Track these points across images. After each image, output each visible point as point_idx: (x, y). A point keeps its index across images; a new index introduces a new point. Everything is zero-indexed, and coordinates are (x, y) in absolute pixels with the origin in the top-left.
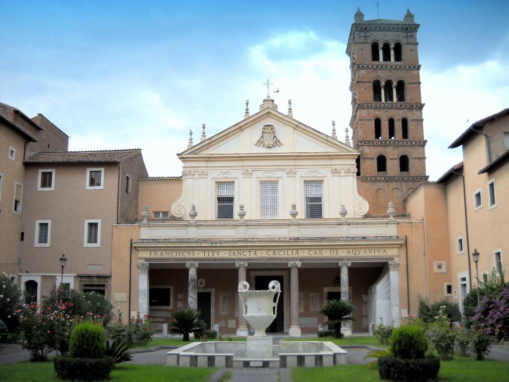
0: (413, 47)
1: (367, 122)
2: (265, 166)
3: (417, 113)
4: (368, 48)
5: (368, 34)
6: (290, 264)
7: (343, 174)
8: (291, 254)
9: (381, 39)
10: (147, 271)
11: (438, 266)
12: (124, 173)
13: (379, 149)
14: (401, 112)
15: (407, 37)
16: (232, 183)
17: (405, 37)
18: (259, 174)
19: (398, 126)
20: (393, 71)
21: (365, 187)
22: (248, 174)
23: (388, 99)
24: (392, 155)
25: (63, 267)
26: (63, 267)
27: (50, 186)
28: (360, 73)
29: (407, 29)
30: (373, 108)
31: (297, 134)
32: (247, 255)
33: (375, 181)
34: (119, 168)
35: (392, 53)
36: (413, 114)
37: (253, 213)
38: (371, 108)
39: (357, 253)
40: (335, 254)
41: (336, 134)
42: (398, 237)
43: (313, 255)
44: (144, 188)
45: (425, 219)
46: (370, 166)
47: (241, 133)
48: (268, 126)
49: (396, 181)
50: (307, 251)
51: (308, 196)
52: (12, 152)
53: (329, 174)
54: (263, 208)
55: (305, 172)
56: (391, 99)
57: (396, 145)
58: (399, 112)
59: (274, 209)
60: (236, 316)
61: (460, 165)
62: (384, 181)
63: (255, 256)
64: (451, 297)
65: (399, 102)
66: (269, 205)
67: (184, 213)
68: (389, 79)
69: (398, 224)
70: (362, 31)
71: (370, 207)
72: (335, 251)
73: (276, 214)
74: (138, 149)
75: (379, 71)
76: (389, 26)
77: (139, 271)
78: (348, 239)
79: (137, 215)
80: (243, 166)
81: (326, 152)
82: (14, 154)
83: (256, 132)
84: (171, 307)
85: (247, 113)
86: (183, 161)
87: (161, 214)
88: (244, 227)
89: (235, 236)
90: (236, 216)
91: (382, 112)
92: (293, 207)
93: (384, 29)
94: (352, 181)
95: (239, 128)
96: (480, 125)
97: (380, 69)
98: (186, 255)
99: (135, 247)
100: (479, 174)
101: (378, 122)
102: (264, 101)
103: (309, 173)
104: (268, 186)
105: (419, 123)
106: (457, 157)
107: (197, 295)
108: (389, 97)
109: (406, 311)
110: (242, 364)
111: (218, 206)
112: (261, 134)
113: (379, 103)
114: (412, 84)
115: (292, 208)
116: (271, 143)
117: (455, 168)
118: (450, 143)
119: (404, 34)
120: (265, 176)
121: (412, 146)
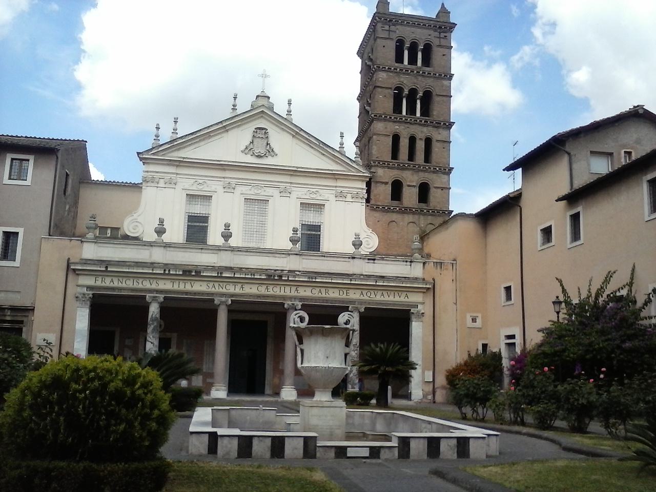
0: (445, 51)
1: (382, 138)
2: (253, 180)
3: (443, 133)
5: (393, 28)
7: (349, 198)
9: (409, 36)
10: (89, 303)
11: (472, 320)
12: (63, 167)
13: (396, 173)
14: (425, 129)
15: (440, 38)
16: (208, 198)
17: (438, 38)
18: (245, 189)
19: (420, 146)
20: (420, 78)
21: (375, 217)
22: (229, 188)
24: (410, 182)
29: (440, 27)
31: (296, 144)
32: (231, 289)
33: (388, 212)
34: (57, 158)
36: (440, 134)
38: (390, 120)
39: (373, 296)
40: (344, 296)
41: (344, 149)
42: (424, 279)
43: (316, 295)
44: (86, 194)
46: (383, 193)
47: (224, 135)
48: (260, 128)
49: (414, 213)
50: (311, 288)
51: (304, 223)
53: (332, 198)
55: (303, 193)
57: (417, 170)
60: (280, 368)
61: (516, 193)
62: (397, 212)
63: (241, 292)
66: (255, 230)
68: (414, 87)
70: (386, 24)
72: (345, 292)
74: (83, 141)
75: (401, 76)
76: (420, 21)
77: (78, 304)
78: (362, 277)
79: (75, 228)
81: (332, 170)
83: (243, 136)
85: (234, 109)
86: (144, 163)
87: (109, 231)
88: (230, 252)
89: (217, 263)
91: (403, 127)
92: (294, 231)
93: (414, 25)
94: (359, 209)
95: (224, 127)
96: (564, 139)
98: (147, 285)
99: (74, 270)
100: (556, 201)
101: (396, 139)
102: (258, 96)
103: (308, 193)
105: (445, 144)
106: (513, 183)
107: (158, 340)
108: (411, 110)
109: (431, 373)
110: (332, 454)
111: (188, 225)
112: (250, 139)
116: (263, 151)
117: (511, 196)
119: (437, 34)
120: (251, 192)
121: (435, 172)
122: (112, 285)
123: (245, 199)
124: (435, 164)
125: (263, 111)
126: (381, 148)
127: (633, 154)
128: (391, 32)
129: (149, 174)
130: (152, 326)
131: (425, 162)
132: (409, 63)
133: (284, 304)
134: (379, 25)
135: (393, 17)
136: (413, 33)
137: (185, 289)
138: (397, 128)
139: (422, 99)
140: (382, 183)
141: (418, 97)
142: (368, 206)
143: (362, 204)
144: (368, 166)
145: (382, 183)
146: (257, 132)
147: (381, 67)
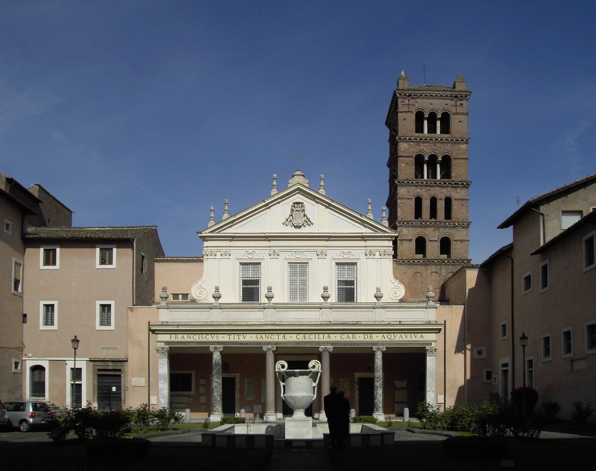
1: (405, 201)
4: (412, 117)
5: (412, 101)
6: (321, 348)
8: (321, 338)
14: (444, 190)
19: (441, 205)
20: (438, 145)
21: (402, 270)
22: (275, 255)
23: (430, 176)
25: (75, 349)
26: (75, 349)
27: (54, 263)
28: (401, 146)
30: (412, 186)
32: (275, 338)
33: (414, 264)
35: (438, 123)
36: (458, 193)
37: (281, 296)
38: (412, 185)
40: (369, 339)
42: (436, 322)
43: (345, 339)
45: (466, 304)
46: (408, 249)
52: (7, 225)
54: (293, 292)
56: (435, 176)
57: (437, 227)
58: (442, 191)
59: (304, 292)
62: (421, 265)
63: (284, 340)
64: (491, 383)
65: (442, 180)
66: (298, 288)
67: (204, 297)
68: (433, 153)
69: (436, 308)
71: (406, 292)
73: (305, 297)
75: (421, 144)
76: (437, 92)
80: (270, 247)
82: (11, 227)
84: (193, 393)
87: (180, 296)
89: (263, 319)
90: (263, 300)
91: (424, 190)
94: (388, 263)
97: (423, 142)
98: (209, 338)
101: (418, 201)
104: (299, 269)
113: (420, 180)
114: (458, 160)
115: (323, 290)
116: (300, 221)
118: (500, 223)
119: (453, 103)
120: (293, 257)
121: (455, 227)
122: (183, 340)
123: (288, 263)
124: (454, 220)
125: (298, 188)
126: (405, 210)
127: (584, 212)
128: (410, 106)
129: (208, 248)
130: (216, 369)
131: (445, 219)
132: (428, 132)
133: (318, 348)
134: (400, 100)
135: (412, 92)
136: (431, 104)
137: (239, 340)
138: (419, 191)
139: (441, 163)
140: (407, 240)
141: (438, 162)
142: (395, 261)
143: (390, 259)
144: (393, 225)
145: (407, 240)
146: (295, 206)
147: (402, 138)
